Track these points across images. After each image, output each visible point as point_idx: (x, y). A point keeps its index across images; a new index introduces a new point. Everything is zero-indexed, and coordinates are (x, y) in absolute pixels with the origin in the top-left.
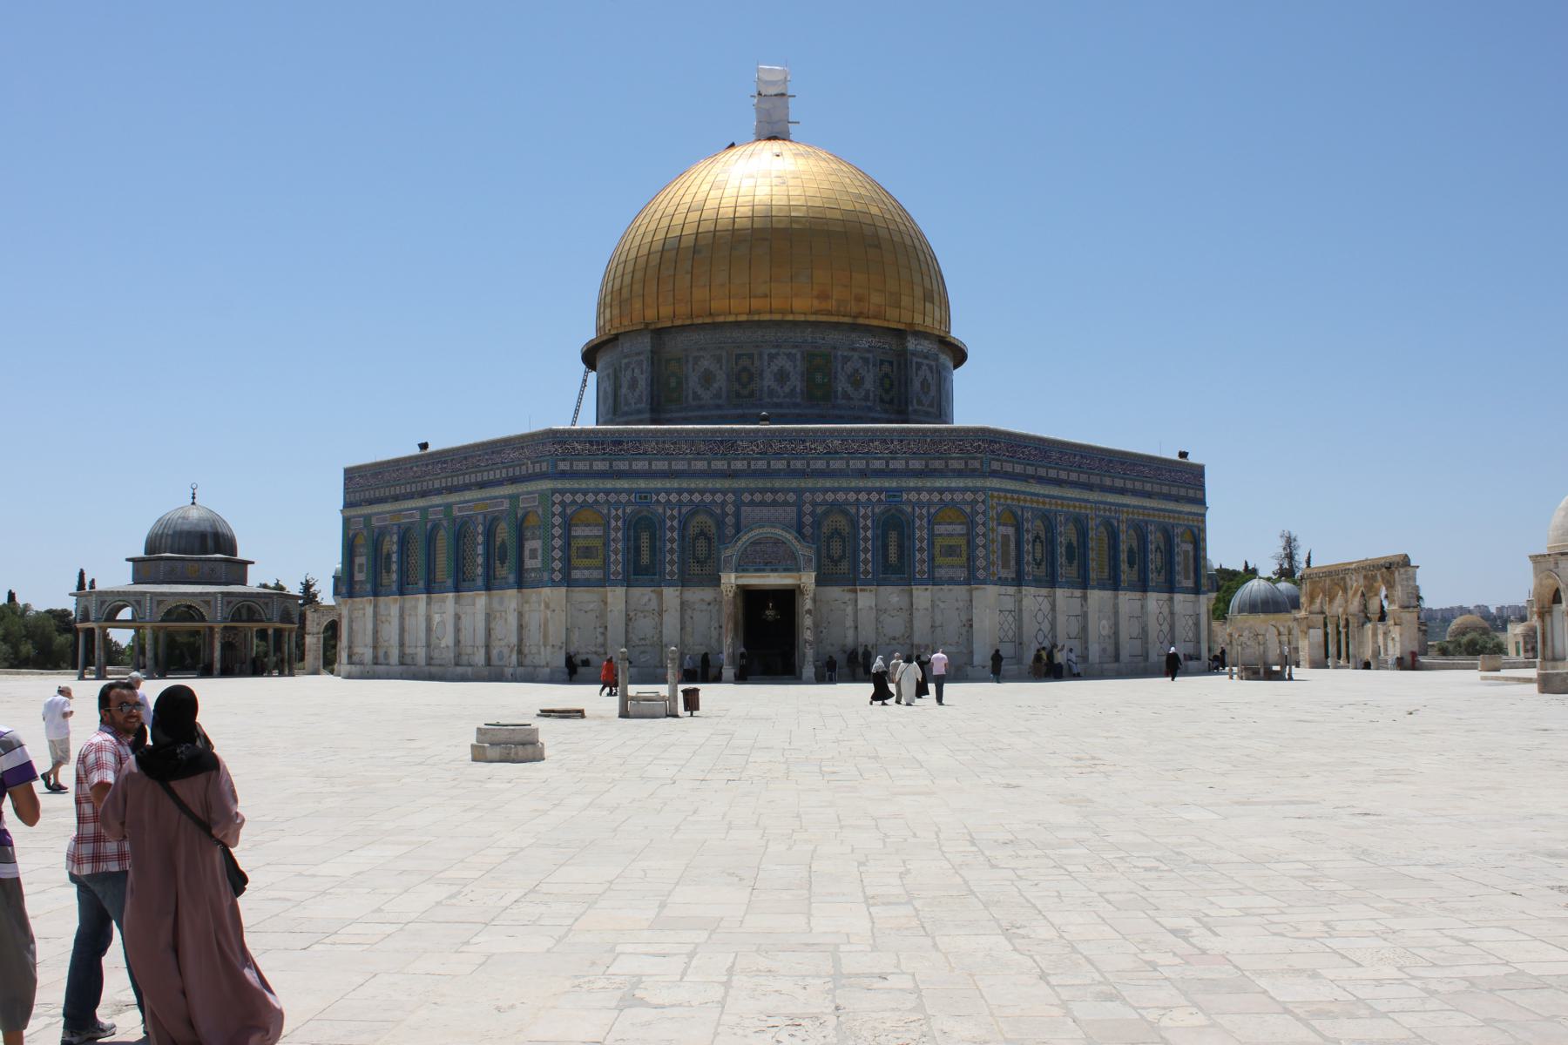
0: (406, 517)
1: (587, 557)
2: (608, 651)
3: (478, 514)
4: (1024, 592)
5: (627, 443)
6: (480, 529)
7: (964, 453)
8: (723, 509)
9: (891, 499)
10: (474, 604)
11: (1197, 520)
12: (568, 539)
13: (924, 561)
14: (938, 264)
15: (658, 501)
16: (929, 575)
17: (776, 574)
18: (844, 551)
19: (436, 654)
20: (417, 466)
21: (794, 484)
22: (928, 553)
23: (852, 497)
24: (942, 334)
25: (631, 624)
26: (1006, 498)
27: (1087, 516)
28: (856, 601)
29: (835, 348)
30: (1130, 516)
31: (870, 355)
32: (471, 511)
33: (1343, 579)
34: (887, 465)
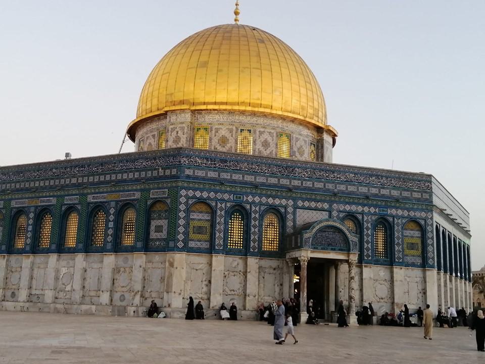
0: (43, 202)
1: (199, 233)
3: (111, 201)
8: (286, 209)
10: (102, 262)
12: (187, 218)
15: (247, 202)
20: (56, 169)
23: (360, 209)
31: (306, 139)
32: (105, 198)
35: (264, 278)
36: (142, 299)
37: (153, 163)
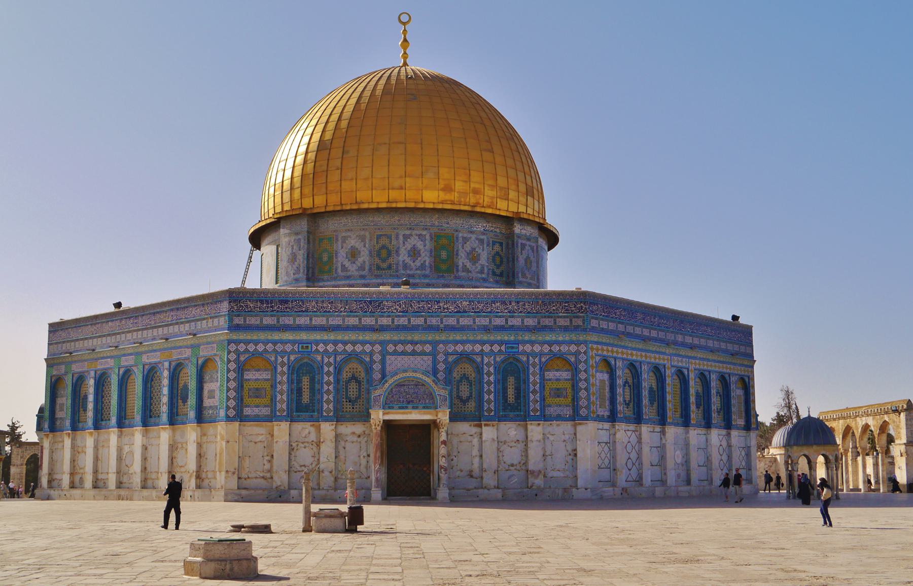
1: (257, 397)
2: (274, 475)
4: (617, 427)
5: (292, 302)
6: (166, 373)
7: (569, 313)
8: (371, 358)
9: (510, 350)
10: (159, 437)
11: (748, 371)
13: (537, 401)
14: (536, 168)
16: (541, 412)
17: (416, 411)
19: (125, 479)
21: (430, 337)
22: (541, 394)
23: (478, 348)
24: (541, 221)
25: (292, 453)
26: (603, 350)
27: (665, 366)
28: (481, 434)
29: (457, 231)
30: (697, 367)
35: (344, 448)
36: (198, 480)
37: (202, 311)
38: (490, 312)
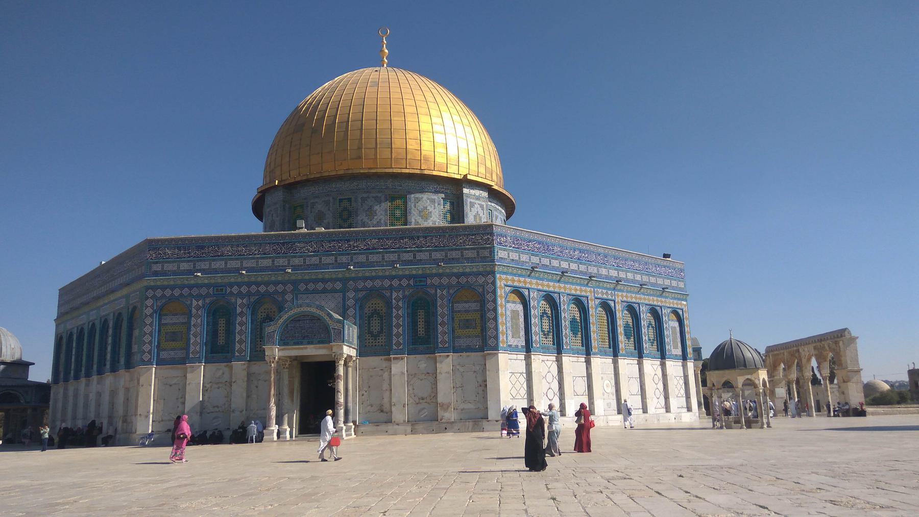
1: (174, 341)
13: (445, 333)
15: (231, 293)
18: (382, 329)
23: (387, 283)
26: (513, 281)
30: (625, 299)
33: (798, 351)
34: (415, 257)
38: (399, 248)
